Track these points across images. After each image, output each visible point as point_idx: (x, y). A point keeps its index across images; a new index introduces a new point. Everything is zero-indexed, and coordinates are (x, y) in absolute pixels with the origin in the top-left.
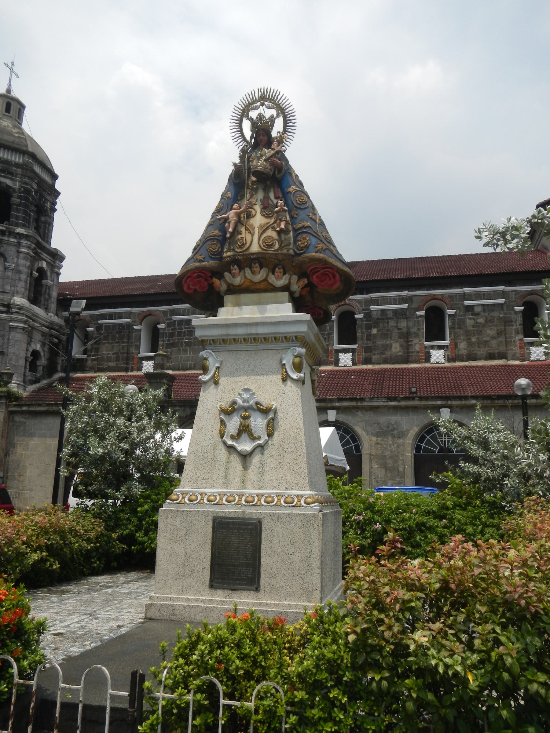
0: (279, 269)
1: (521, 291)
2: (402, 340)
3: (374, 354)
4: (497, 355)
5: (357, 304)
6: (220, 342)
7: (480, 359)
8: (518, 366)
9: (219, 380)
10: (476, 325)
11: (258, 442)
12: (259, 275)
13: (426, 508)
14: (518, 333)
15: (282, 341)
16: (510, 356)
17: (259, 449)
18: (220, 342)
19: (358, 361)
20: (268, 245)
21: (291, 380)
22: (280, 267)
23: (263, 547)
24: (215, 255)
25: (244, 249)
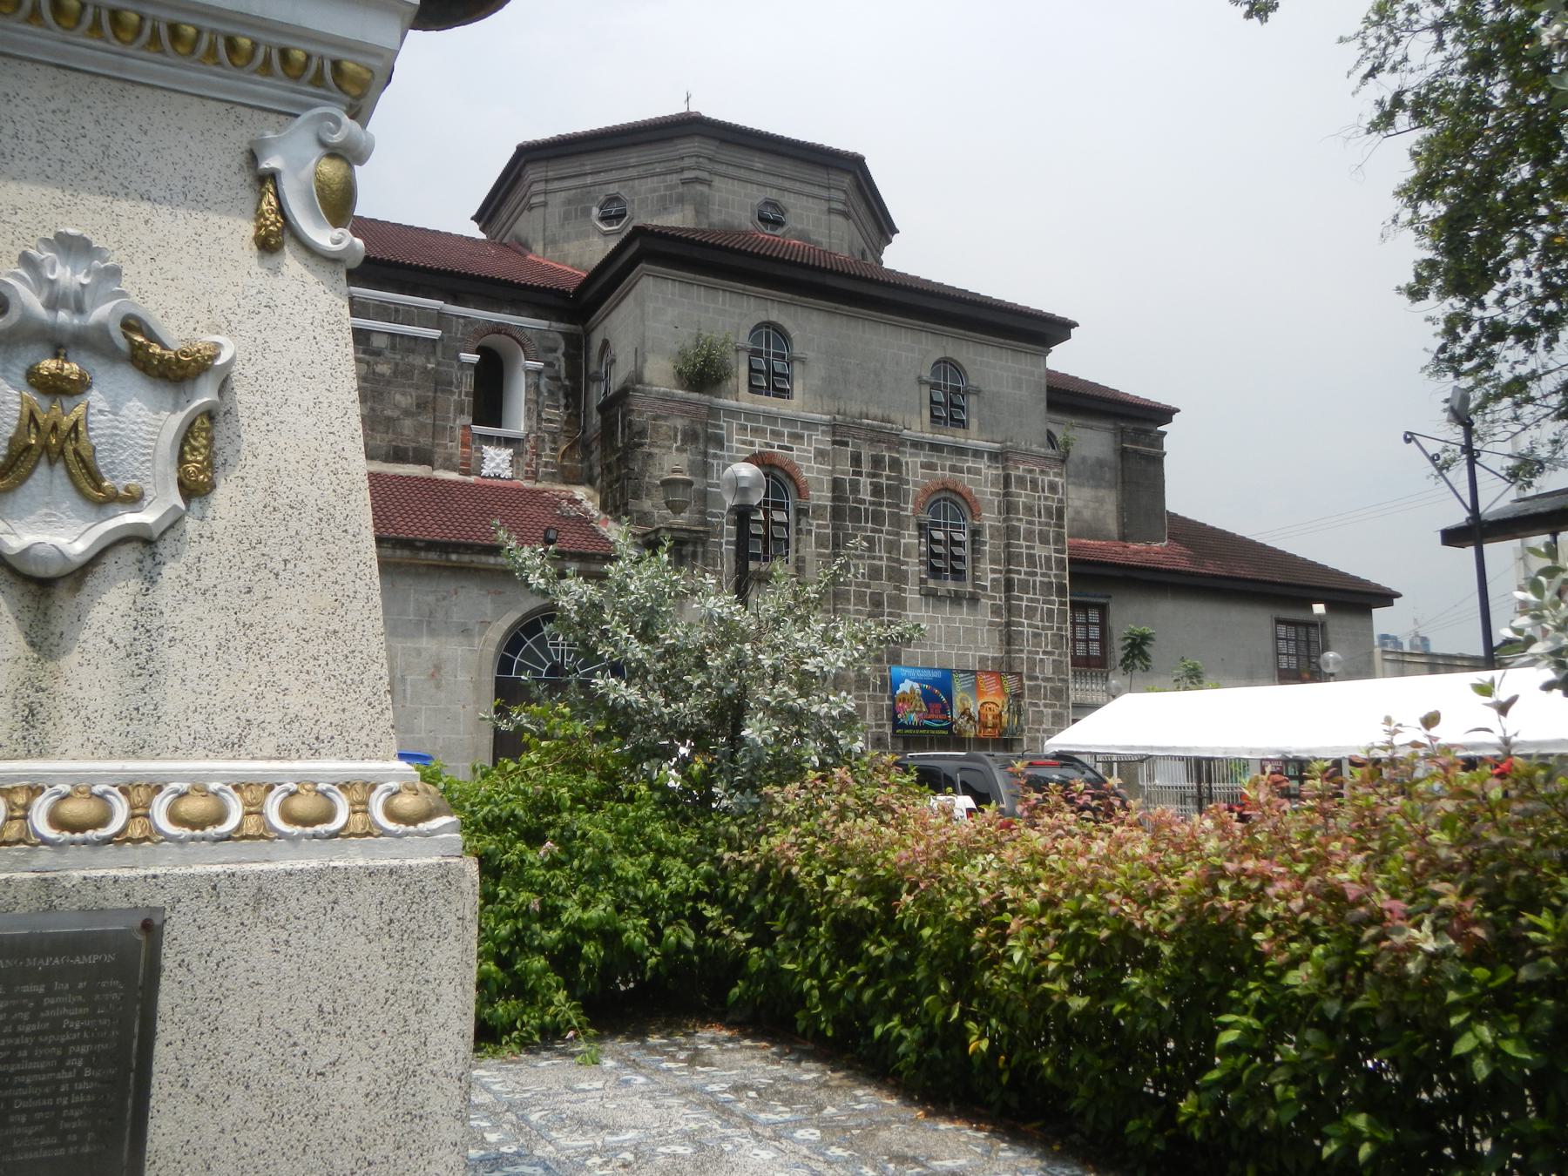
8: (456, 483)
11: (130, 518)
13: (486, 809)
14: (462, 412)
17: (128, 554)
21: (303, 254)
23: (163, 1056)
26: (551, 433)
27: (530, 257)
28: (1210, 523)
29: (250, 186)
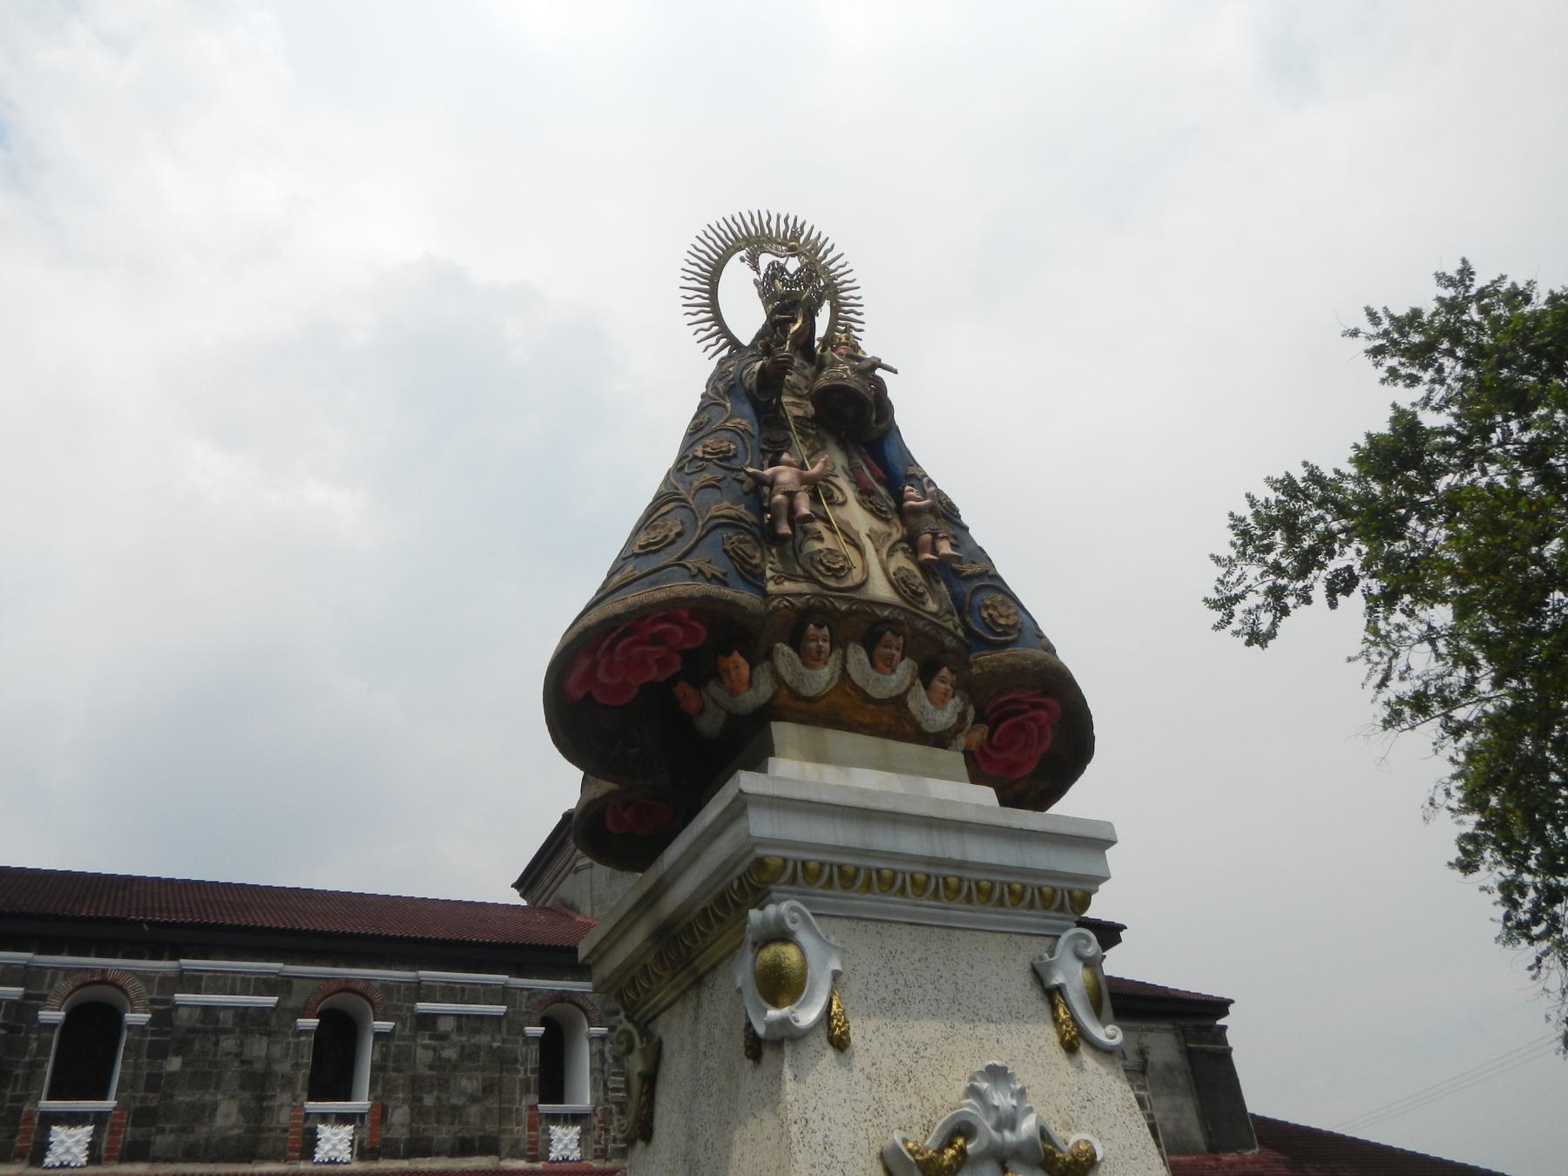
0: (952, 672)
1: (540, 991)
2: (247, 1095)
3: (162, 1131)
4: (477, 1145)
5: (138, 983)
6: (831, 878)
7: (438, 1154)
9: (846, 1033)
10: (439, 1064)
12: (894, 677)
14: (527, 1090)
15: (1031, 905)
16: (507, 1149)
18: (831, 878)
19: (109, 1149)
20: (914, 592)
21: (1092, 1051)
22: (955, 668)
24: (754, 576)
25: (849, 583)
26: (617, 1103)
27: (579, 918)
28: (1292, 1120)
29: (1042, 999)
